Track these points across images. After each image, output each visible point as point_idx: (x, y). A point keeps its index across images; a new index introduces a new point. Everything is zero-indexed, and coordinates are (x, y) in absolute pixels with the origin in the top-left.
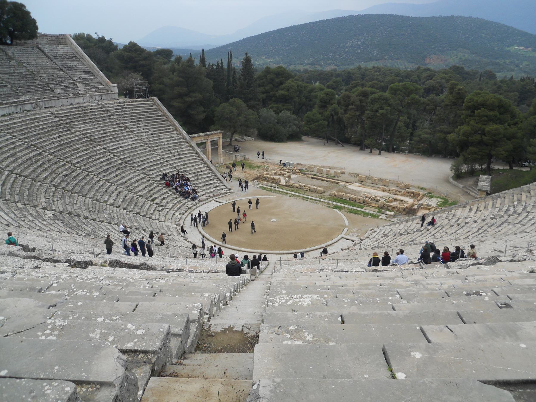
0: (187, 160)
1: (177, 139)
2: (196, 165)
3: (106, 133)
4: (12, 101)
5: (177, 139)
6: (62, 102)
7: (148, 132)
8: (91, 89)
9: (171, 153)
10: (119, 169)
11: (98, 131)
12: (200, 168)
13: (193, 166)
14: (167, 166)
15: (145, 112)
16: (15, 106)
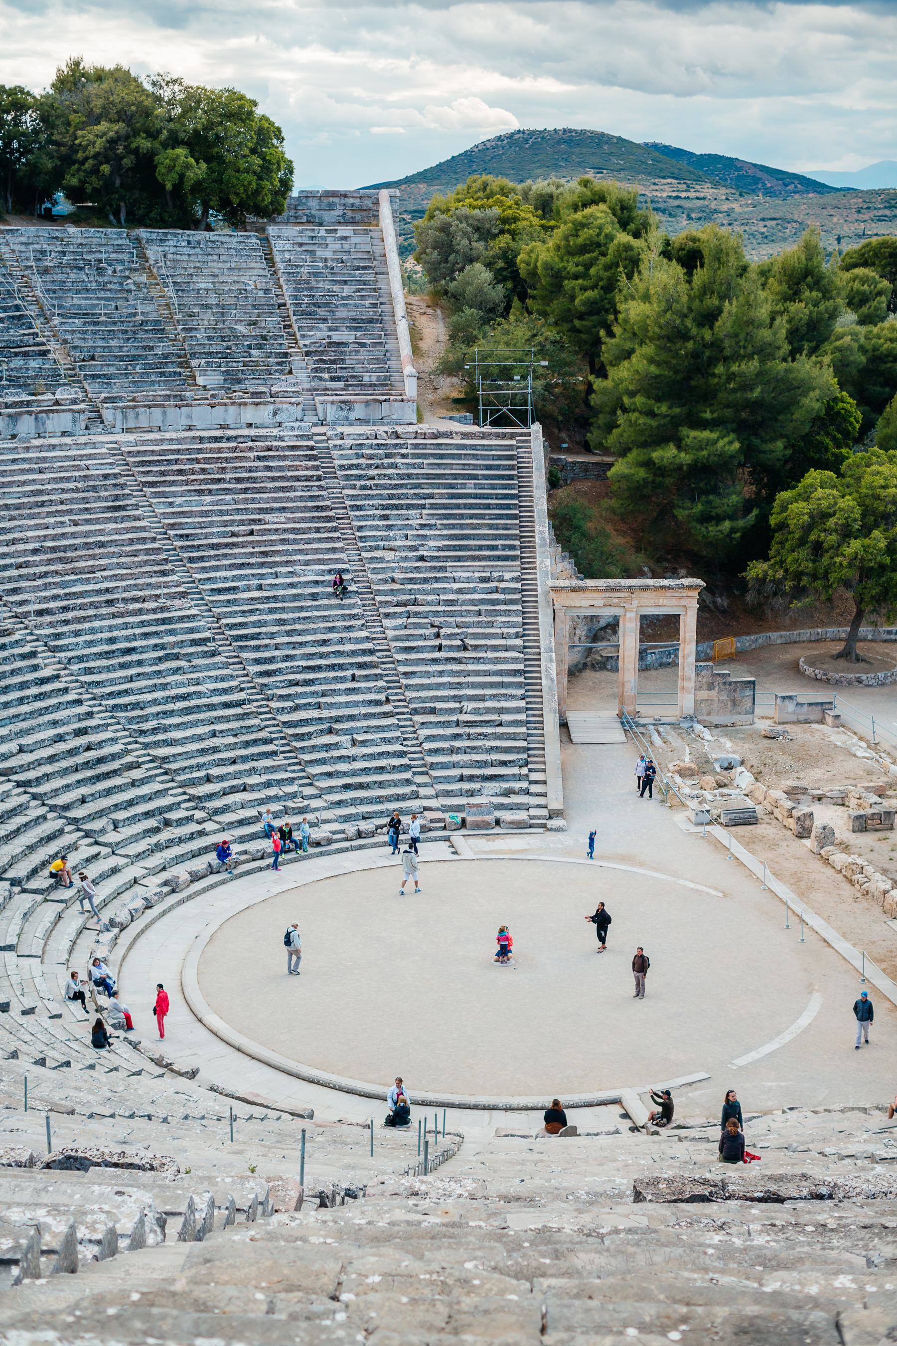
0: (477, 673)
1: (505, 591)
2: (494, 697)
3: (251, 533)
4: (10, 399)
5: (505, 591)
6: (189, 417)
7: (414, 549)
8: (332, 379)
9: (438, 636)
10: (177, 657)
11: (225, 524)
12: (501, 711)
13: (482, 698)
14: (377, 677)
15: (463, 476)
16: (10, 416)
